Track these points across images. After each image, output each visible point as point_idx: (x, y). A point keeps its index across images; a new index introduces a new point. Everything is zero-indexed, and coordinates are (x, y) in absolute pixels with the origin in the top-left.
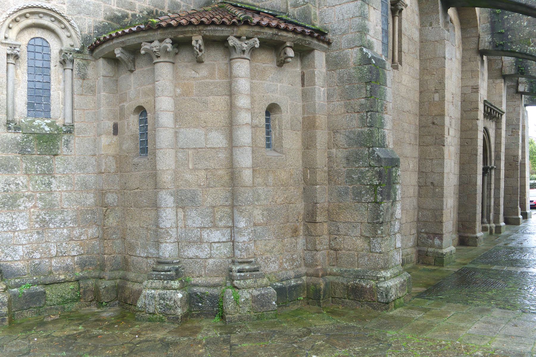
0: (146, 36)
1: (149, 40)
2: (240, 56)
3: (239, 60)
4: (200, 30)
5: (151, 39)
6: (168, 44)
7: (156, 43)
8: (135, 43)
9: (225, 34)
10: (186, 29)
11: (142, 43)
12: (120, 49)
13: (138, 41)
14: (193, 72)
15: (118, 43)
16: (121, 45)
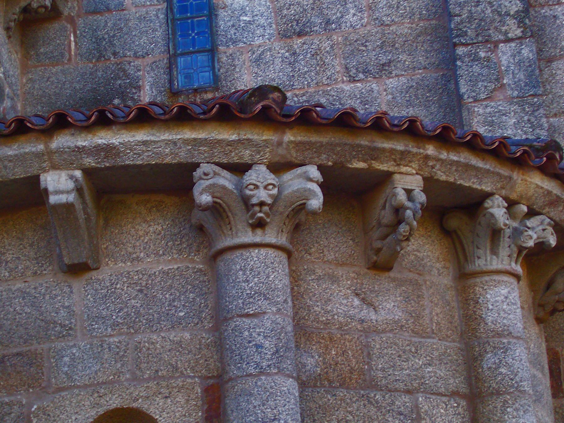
0: (230, 143)
1: (236, 160)
2: (508, 268)
3: (505, 278)
4: (427, 157)
5: (246, 155)
6: (306, 184)
7: (260, 175)
8: (168, 160)
9: (487, 187)
10: (387, 145)
11: (197, 165)
12: (78, 174)
13: (183, 156)
14: (357, 302)
15: (80, 150)
16: (90, 162)
